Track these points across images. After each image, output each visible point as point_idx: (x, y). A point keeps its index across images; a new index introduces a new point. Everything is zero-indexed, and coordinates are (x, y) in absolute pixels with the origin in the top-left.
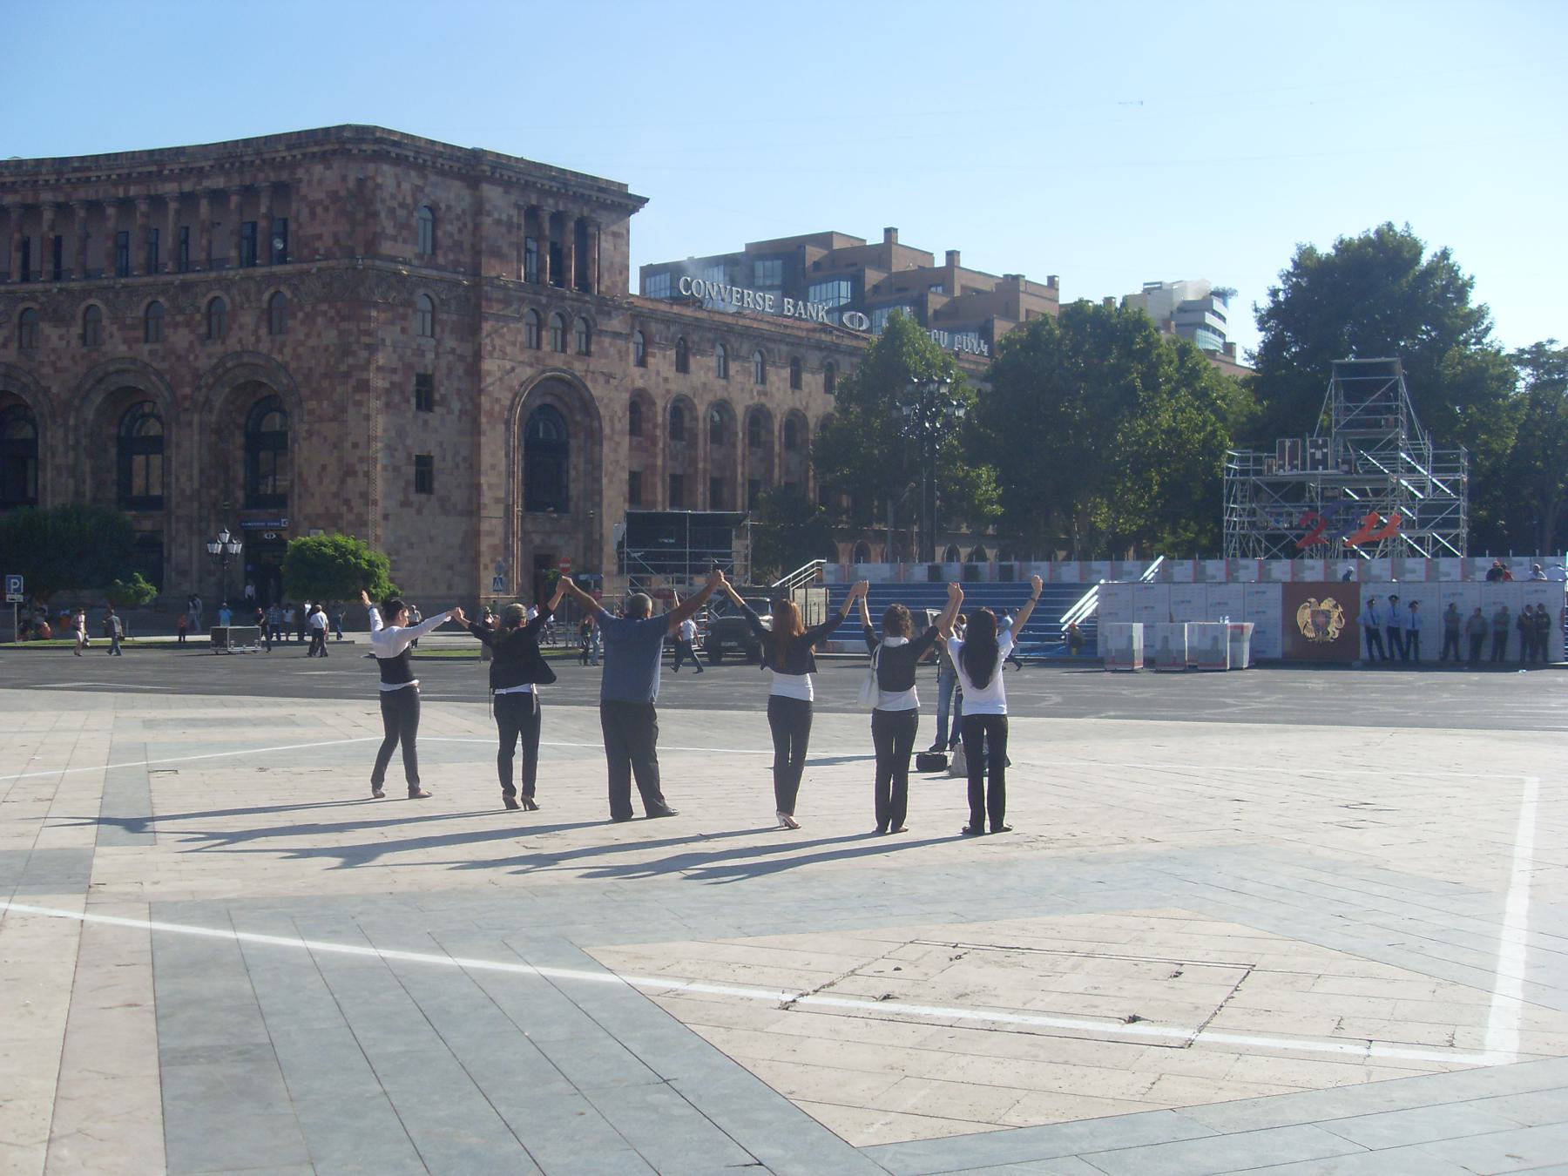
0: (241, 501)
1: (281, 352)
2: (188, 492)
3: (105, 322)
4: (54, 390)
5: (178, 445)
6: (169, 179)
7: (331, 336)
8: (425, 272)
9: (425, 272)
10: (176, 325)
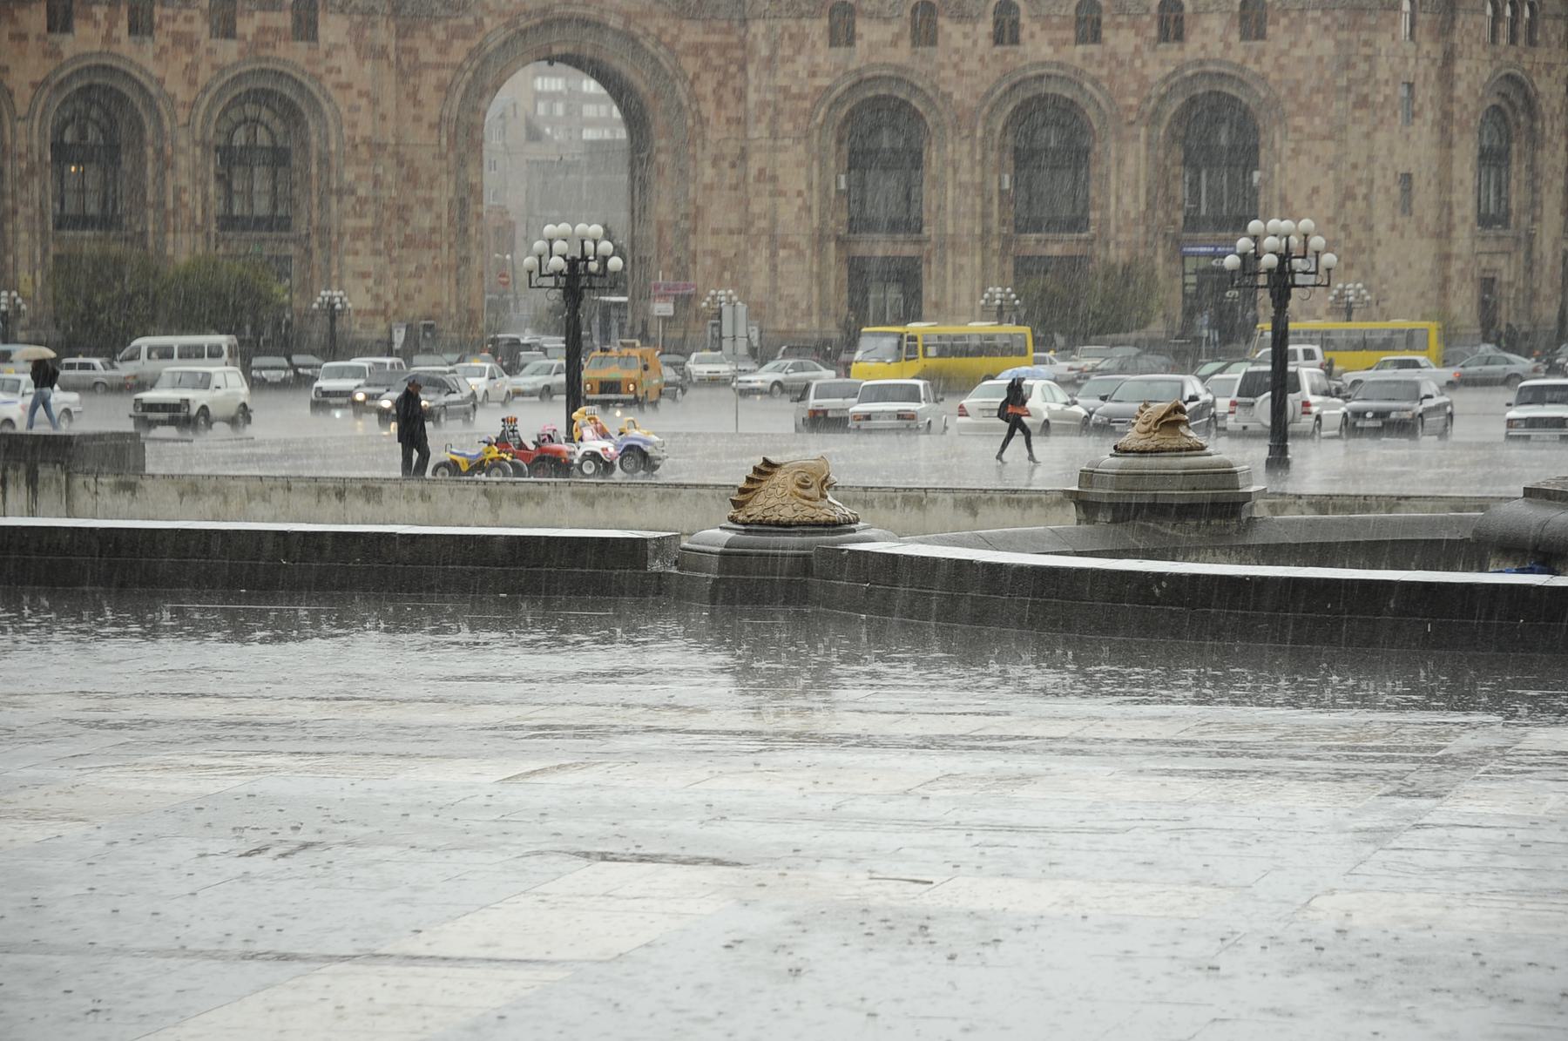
0: (1181, 223)
1: (1258, 61)
2: (1132, 215)
3: (1023, 20)
4: (957, 96)
5: (1120, 162)
7: (1326, 46)
10: (1119, 26)
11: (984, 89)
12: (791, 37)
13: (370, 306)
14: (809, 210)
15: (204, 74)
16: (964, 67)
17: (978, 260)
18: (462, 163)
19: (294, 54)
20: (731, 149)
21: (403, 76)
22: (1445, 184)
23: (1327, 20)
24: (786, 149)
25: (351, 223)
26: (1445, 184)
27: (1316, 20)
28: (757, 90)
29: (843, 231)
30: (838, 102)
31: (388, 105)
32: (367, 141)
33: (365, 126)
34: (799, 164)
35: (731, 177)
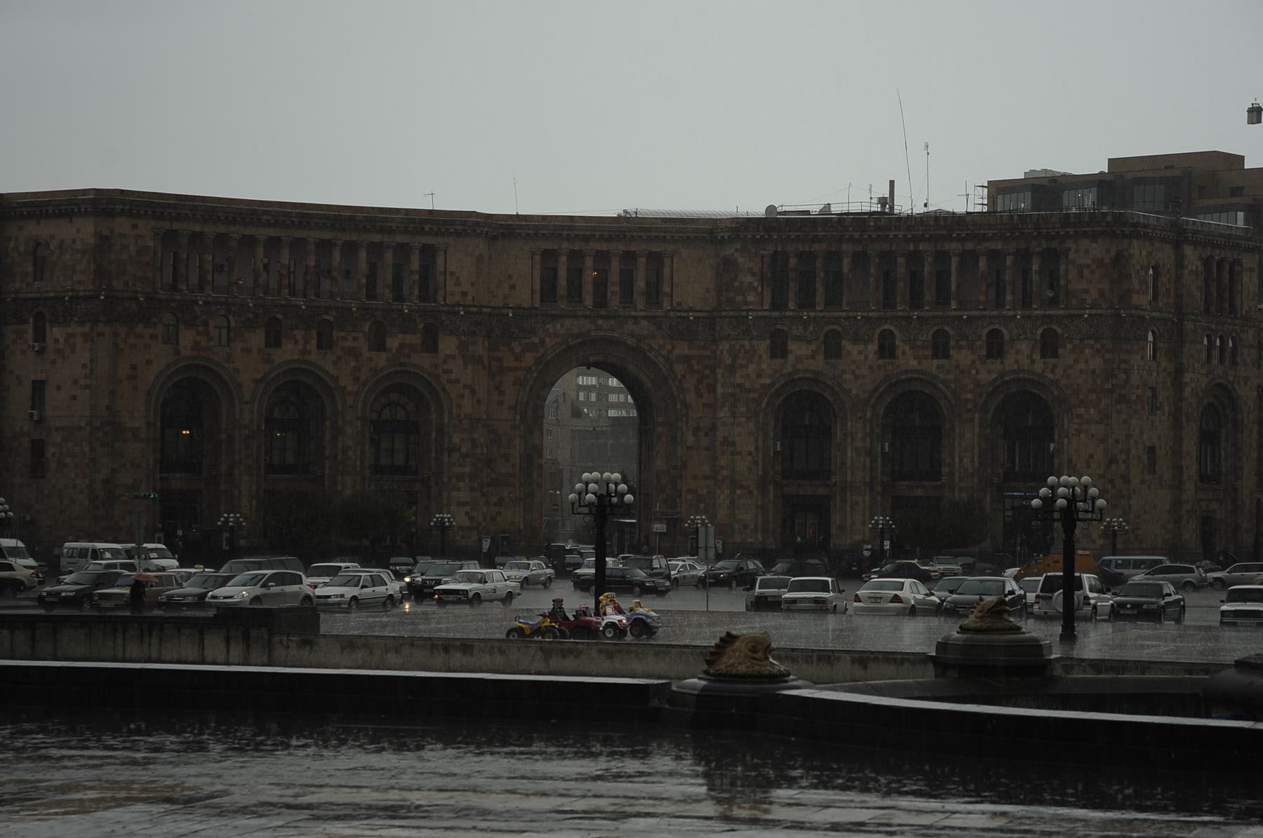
1: (1053, 372)
2: (970, 470)
4: (854, 391)
7: (1097, 363)
8: (1154, 314)
9: (1154, 314)
10: (961, 347)
12: (746, 352)
13: (468, 524)
17: (867, 498)
23: (1098, 346)
27: (1092, 346)
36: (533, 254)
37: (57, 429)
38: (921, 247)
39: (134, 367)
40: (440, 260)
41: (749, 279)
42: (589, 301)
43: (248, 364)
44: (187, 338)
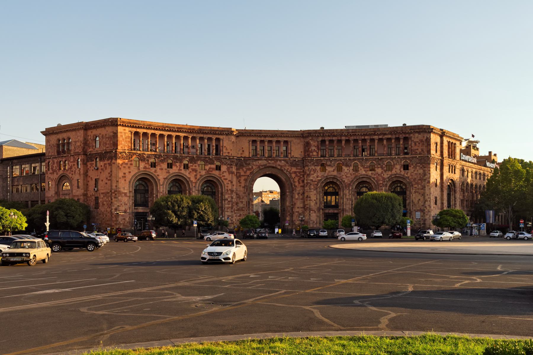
6: (376, 135)
10: (378, 168)
11: (351, 180)
14: (317, 203)
15: (198, 177)
16: (347, 174)
18: (249, 194)
19: (217, 173)
20: (301, 192)
21: (237, 177)
22: (442, 199)
24: (311, 192)
25: (227, 206)
26: (442, 199)
28: (307, 180)
29: (323, 208)
30: (323, 182)
31: (234, 183)
32: (230, 190)
33: (230, 188)
34: (315, 194)
35: (301, 197)
36: (249, 141)
37: (102, 193)
38: (366, 137)
39: (125, 174)
40: (221, 142)
41: (314, 148)
42: (266, 155)
43: (162, 175)
44: (142, 165)
